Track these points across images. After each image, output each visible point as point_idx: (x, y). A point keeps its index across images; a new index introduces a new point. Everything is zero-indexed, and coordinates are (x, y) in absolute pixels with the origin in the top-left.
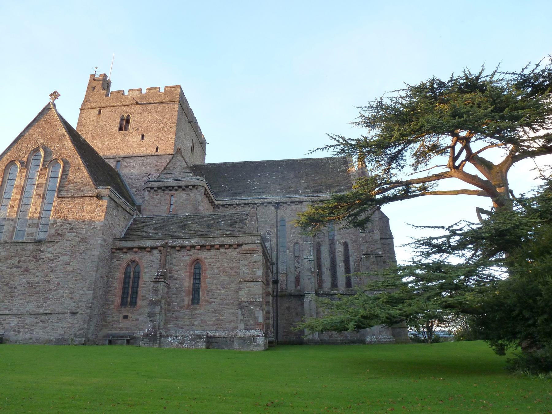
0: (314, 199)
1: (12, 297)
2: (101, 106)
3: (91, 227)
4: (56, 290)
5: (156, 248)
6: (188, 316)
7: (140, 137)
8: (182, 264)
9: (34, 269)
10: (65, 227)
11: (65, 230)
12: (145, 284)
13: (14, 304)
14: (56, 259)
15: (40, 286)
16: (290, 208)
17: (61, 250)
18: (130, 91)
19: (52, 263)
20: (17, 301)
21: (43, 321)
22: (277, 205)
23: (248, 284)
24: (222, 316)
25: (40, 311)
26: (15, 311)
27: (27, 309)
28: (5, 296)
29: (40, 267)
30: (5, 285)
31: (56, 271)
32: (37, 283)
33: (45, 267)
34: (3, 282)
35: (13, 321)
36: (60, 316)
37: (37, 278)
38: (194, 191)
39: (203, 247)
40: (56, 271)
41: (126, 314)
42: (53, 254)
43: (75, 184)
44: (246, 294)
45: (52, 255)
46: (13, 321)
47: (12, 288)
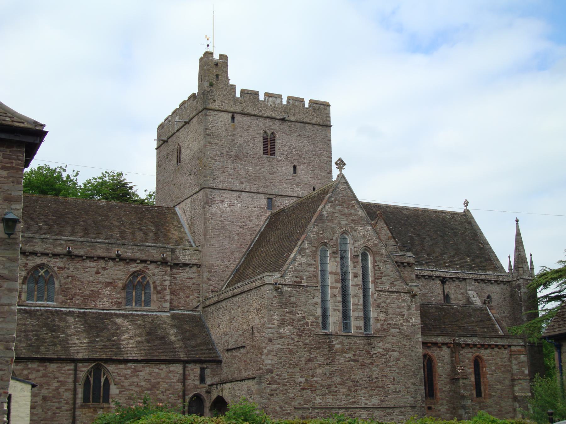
0: (478, 277)
1: (356, 390)
2: (232, 110)
3: (411, 324)
4: (394, 385)
5: (446, 344)
6: (478, 407)
7: (292, 168)
8: (467, 361)
9: (369, 364)
10: (388, 322)
11: (389, 326)
12: (441, 378)
13: (360, 397)
14: (387, 354)
15: (379, 381)
16: (454, 284)
17: (390, 346)
18: (267, 95)
19: (385, 359)
20: (362, 395)
21: (389, 414)
22: (443, 281)
23: (520, 381)
24: (502, 407)
25: (385, 404)
26: (363, 405)
27: (373, 402)
28: (350, 390)
29: (375, 362)
30: (348, 379)
31: (390, 366)
32: (375, 378)
33: (379, 362)
34: (345, 376)
35: (363, 414)
36: (403, 410)
37: (375, 373)
38: (408, 269)
39: (483, 345)
40: (390, 366)
41: (430, 406)
42: (384, 349)
43: (388, 277)
44: (519, 390)
45: (383, 350)
46: (363, 414)
47: (354, 382)
